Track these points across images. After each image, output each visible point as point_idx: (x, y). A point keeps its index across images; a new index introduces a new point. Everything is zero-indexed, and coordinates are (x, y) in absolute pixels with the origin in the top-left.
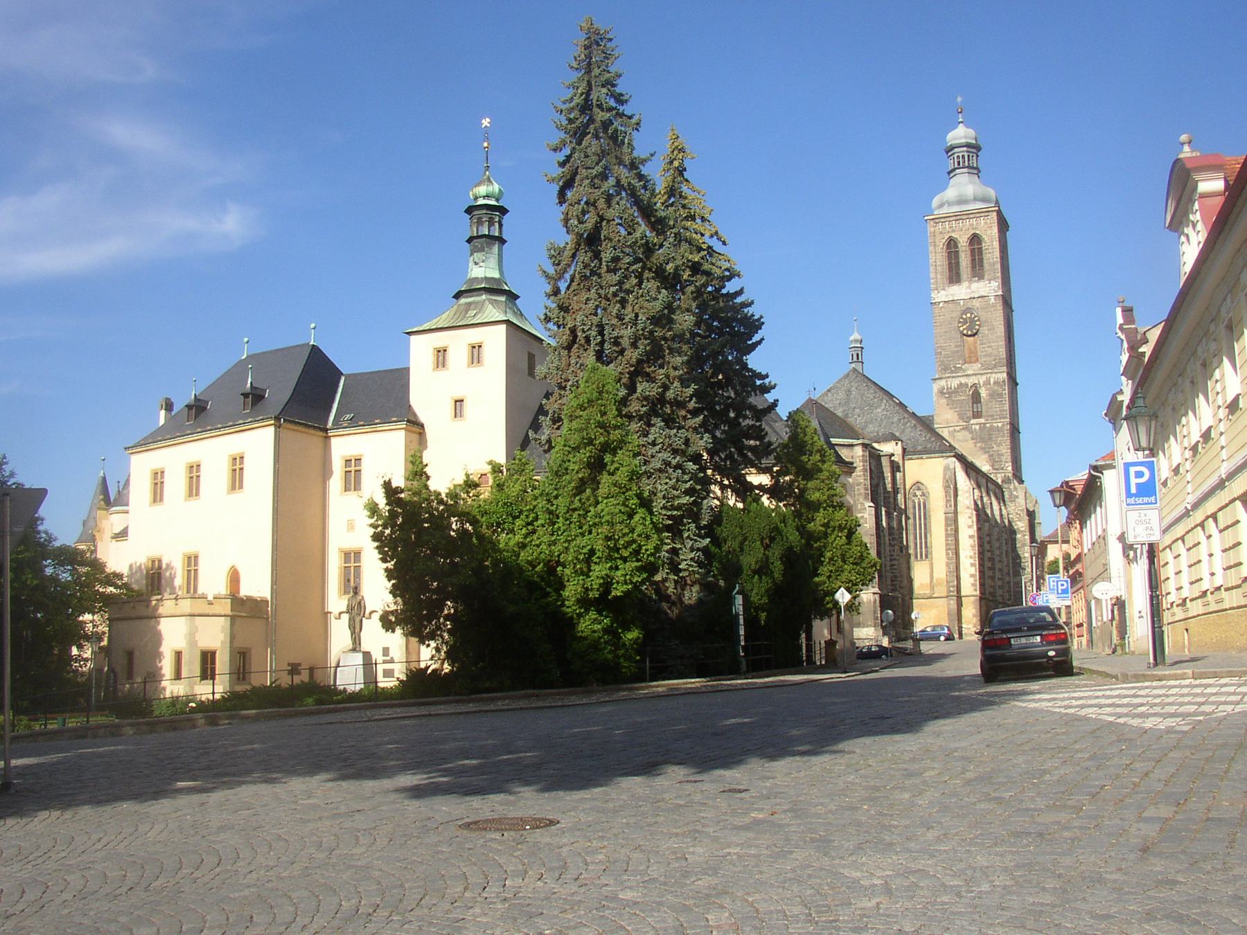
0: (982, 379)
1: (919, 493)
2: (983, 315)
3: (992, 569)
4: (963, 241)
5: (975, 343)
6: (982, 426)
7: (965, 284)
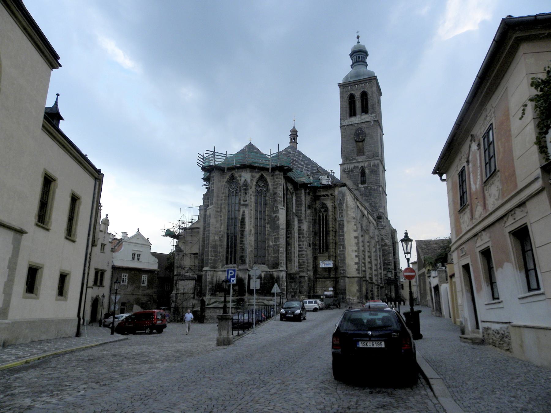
0: (366, 164)
1: (323, 210)
2: (367, 131)
3: (370, 262)
4: (358, 95)
5: (363, 145)
6: (366, 188)
7: (358, 116)
